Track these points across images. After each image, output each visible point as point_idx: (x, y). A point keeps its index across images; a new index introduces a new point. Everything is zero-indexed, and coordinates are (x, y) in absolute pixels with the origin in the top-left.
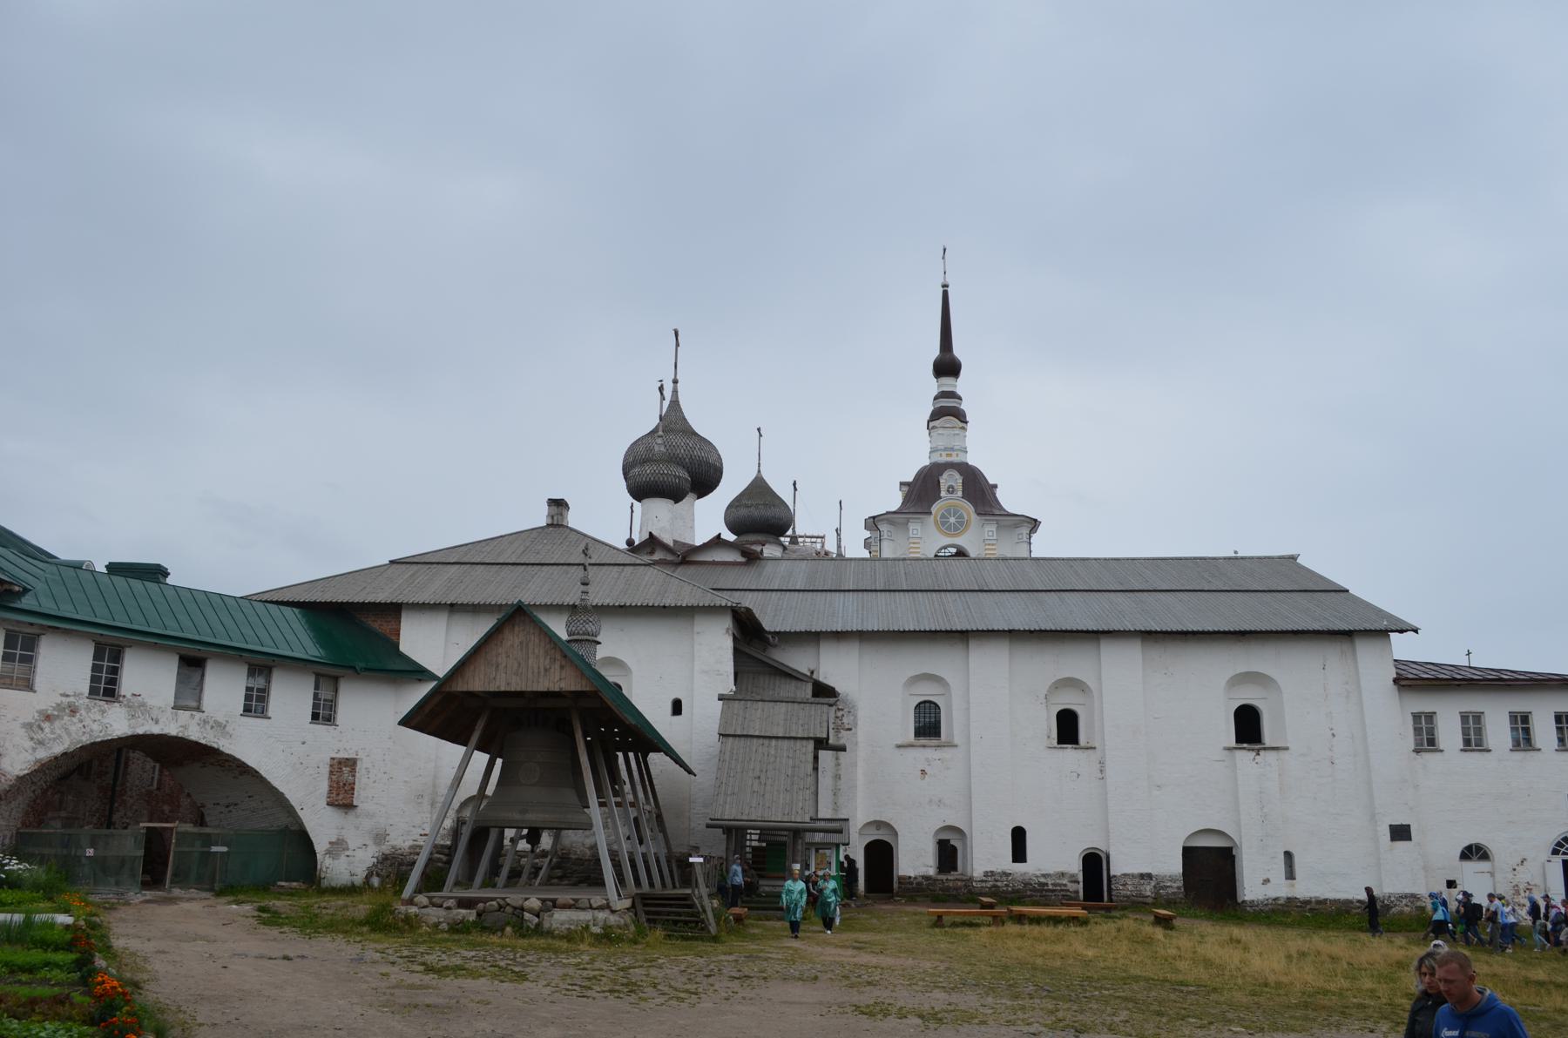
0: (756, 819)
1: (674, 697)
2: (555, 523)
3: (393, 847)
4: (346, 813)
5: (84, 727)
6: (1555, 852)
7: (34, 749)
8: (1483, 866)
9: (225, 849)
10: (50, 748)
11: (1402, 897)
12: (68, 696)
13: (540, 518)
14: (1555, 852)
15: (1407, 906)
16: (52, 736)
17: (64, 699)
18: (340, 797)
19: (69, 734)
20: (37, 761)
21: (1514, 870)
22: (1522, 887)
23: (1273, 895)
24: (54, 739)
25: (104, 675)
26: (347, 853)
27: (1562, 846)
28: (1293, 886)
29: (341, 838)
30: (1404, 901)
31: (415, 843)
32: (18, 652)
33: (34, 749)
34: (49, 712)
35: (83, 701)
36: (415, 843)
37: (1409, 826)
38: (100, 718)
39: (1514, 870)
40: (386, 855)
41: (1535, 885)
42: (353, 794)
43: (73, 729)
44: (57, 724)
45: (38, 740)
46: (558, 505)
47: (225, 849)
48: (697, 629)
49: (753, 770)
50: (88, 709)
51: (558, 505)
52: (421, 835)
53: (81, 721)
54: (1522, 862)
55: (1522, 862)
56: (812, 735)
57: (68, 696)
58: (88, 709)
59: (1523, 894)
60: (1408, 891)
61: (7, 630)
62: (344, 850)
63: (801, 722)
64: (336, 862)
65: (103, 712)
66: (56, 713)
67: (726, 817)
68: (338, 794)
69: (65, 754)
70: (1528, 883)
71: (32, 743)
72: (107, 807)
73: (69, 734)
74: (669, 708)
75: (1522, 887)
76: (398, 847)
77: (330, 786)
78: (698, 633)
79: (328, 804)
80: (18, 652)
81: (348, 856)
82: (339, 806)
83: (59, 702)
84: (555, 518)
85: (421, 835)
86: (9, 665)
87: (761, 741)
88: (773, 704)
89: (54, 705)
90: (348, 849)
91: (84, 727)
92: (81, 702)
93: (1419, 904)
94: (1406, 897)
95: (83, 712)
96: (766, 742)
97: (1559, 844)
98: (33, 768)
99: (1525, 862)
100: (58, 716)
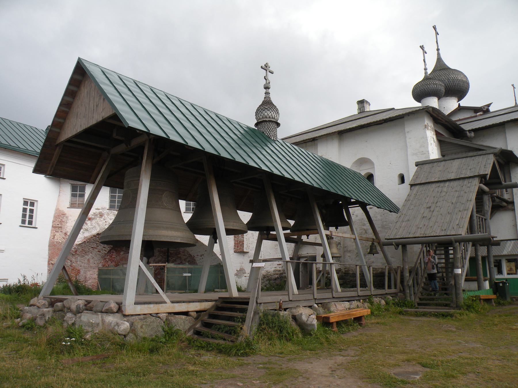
0: (419, 236)
1: (399, 174)
2: (361, 111)
3: (267, 271)
4: (244, 256)
5: (106, 222)
9: (190, 275)
10: (91, 232)
12: (99, 209)
13: (354, 110)
16: (92, 227)
17: (97, 211)
18: (239, 248)
19: (99, 225)
20: (85, 238)
24: (92, 228)
25: (117, 199)
26: (245, 275)
29: (242, 268)
31: (276, 269)
32: (78, 193)
35: (105, 211)
36: (276, 269)
40: (264, 275)
42: (243, 246)
43: (100, 223)
44: (94, 221)
46: (361, 103)
47: (190, 275)
48: (407, 130)
49: (428, 202)
50: (108, 214)
51: (361, 103)
52: (278, 265)
53: (104, 219)
56: (477, 174)
57: (99, 209)
58: (108, 214)
61: (72, 184)
62: (243, 273)
63: (470, 168)
64: (240, 279)
66: (93, 217)
67: (397, 237)
68: (238, 247)
69: (98, 234)
72: (166, 259)
73: (99, 225)
74: (397, 180)
76: (269, 271)
77: (235, 243)
78: (408, 132)
79: (234, 252)
80: (78, 193)
81: (245, 276)
82: (238, 252)
83: (95, 212)
84: (361, 109)
85: (278, 265)
86: (75, 199)
87: (438, 185)
88: (452, 161)
90: (245, 273)
91: (106, 222)
92: (105, 211)
95: (106, 216)
96: (442, 184)
98: (83, 241)
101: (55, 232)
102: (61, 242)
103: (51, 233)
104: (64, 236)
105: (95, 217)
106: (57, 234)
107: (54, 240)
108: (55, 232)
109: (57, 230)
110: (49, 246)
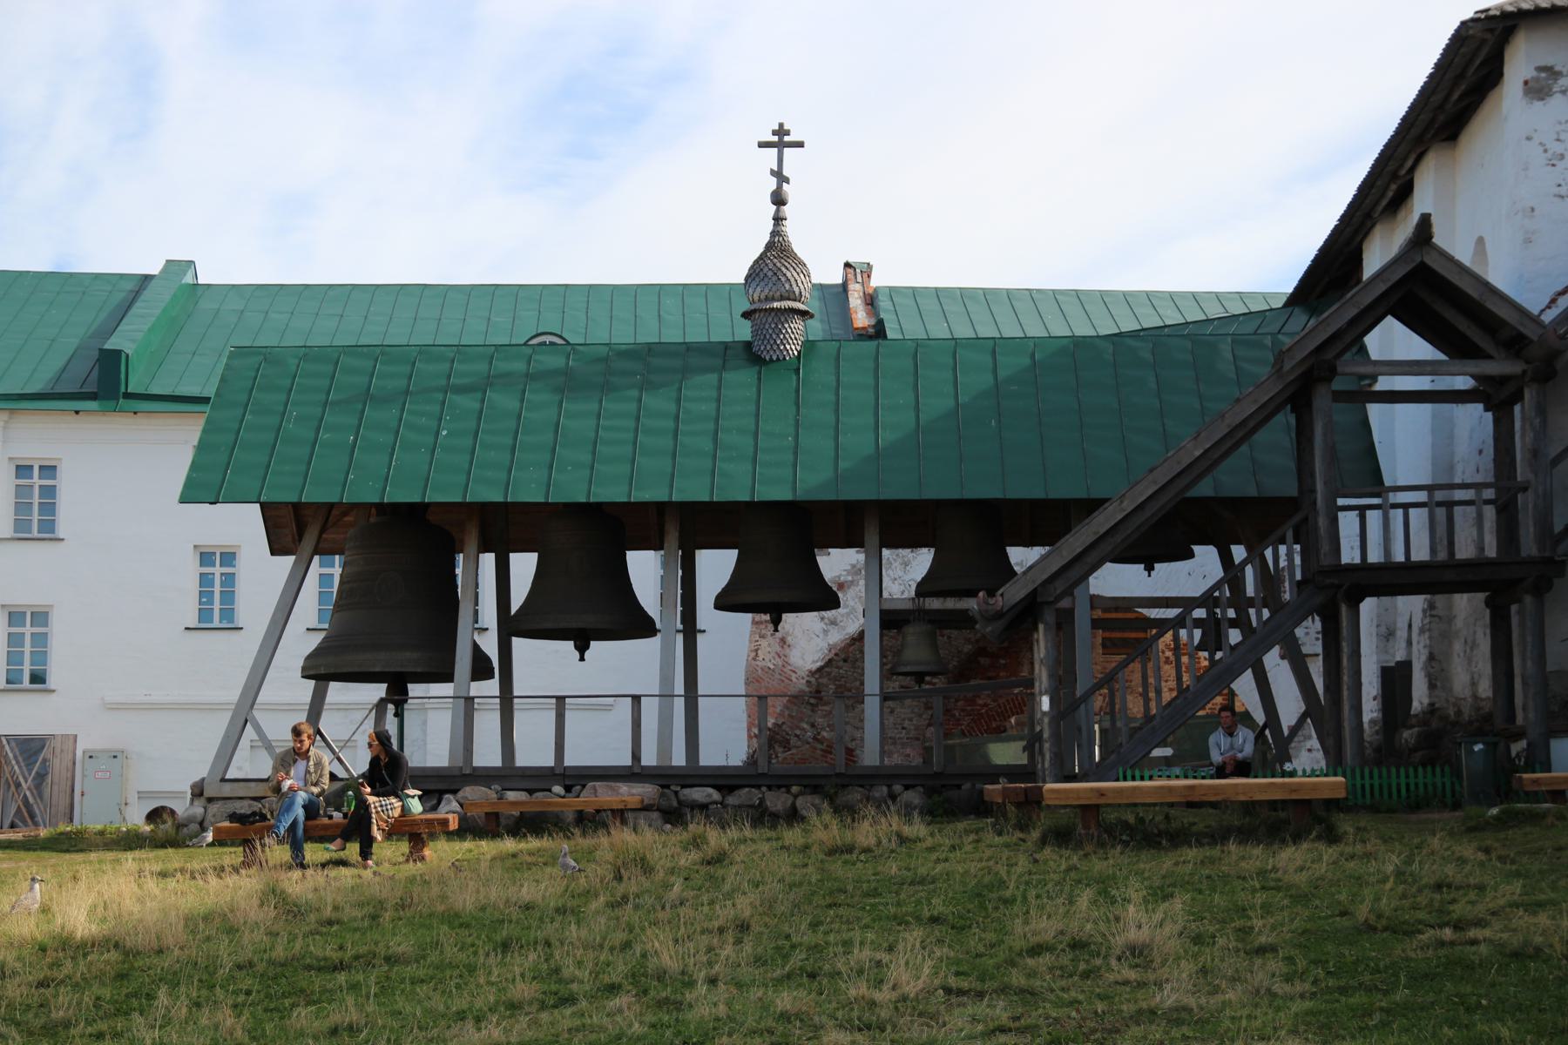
7: (826, 632)
10: (844, 628)
33: (826, 632)
34: (842, 578)
38: (901, 573)
45: (828, 619)
65: (906, 564)
66: (850, 578)
71: (822, 625)
83: (854, 562)
89: (849, 568)
98: (827, 658)
100: (852, 582)
101: (757, 638)
102: (772, 667)
103: (750, 642)
104: (778, 649)
105: (855, 578)
106: (764, 643)
107: (758, 663)
108: (757, 638)
109: (763, 632)
110: (746, 684)
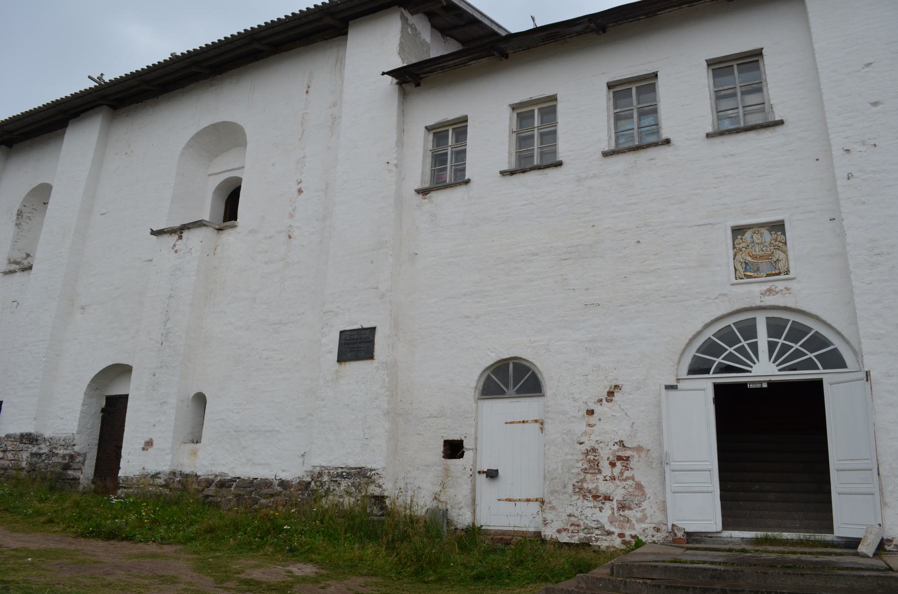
6: (698, 368)
8: (526, 407)
11: (341, 475)
14: (698, 368)
15: (349, 494)
21: (591, 412)
22: (606, 453)
23: (152, 468)
27: (732, 340)
28: (195, 453)
30: (344, 484)
37: (341, 332)
39: (591, 412)
41: (639, 449)
54: (611, 394)
55: (611, 394)
59: (607, 470)
60: (353, 462)
70: (621, 443)
75: (606, 453)
93: (373, 490)
94: (349, 475)
97: (710, 348)
99: (617, 396)
